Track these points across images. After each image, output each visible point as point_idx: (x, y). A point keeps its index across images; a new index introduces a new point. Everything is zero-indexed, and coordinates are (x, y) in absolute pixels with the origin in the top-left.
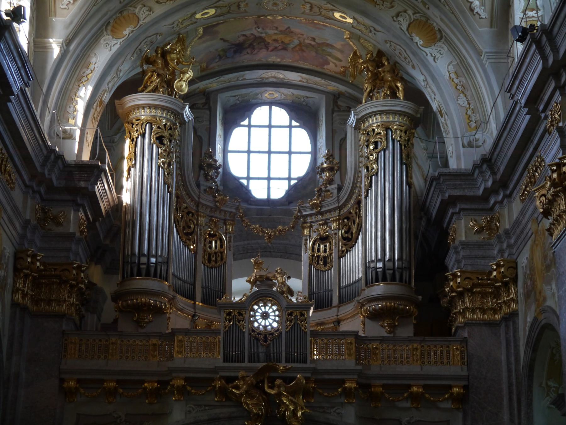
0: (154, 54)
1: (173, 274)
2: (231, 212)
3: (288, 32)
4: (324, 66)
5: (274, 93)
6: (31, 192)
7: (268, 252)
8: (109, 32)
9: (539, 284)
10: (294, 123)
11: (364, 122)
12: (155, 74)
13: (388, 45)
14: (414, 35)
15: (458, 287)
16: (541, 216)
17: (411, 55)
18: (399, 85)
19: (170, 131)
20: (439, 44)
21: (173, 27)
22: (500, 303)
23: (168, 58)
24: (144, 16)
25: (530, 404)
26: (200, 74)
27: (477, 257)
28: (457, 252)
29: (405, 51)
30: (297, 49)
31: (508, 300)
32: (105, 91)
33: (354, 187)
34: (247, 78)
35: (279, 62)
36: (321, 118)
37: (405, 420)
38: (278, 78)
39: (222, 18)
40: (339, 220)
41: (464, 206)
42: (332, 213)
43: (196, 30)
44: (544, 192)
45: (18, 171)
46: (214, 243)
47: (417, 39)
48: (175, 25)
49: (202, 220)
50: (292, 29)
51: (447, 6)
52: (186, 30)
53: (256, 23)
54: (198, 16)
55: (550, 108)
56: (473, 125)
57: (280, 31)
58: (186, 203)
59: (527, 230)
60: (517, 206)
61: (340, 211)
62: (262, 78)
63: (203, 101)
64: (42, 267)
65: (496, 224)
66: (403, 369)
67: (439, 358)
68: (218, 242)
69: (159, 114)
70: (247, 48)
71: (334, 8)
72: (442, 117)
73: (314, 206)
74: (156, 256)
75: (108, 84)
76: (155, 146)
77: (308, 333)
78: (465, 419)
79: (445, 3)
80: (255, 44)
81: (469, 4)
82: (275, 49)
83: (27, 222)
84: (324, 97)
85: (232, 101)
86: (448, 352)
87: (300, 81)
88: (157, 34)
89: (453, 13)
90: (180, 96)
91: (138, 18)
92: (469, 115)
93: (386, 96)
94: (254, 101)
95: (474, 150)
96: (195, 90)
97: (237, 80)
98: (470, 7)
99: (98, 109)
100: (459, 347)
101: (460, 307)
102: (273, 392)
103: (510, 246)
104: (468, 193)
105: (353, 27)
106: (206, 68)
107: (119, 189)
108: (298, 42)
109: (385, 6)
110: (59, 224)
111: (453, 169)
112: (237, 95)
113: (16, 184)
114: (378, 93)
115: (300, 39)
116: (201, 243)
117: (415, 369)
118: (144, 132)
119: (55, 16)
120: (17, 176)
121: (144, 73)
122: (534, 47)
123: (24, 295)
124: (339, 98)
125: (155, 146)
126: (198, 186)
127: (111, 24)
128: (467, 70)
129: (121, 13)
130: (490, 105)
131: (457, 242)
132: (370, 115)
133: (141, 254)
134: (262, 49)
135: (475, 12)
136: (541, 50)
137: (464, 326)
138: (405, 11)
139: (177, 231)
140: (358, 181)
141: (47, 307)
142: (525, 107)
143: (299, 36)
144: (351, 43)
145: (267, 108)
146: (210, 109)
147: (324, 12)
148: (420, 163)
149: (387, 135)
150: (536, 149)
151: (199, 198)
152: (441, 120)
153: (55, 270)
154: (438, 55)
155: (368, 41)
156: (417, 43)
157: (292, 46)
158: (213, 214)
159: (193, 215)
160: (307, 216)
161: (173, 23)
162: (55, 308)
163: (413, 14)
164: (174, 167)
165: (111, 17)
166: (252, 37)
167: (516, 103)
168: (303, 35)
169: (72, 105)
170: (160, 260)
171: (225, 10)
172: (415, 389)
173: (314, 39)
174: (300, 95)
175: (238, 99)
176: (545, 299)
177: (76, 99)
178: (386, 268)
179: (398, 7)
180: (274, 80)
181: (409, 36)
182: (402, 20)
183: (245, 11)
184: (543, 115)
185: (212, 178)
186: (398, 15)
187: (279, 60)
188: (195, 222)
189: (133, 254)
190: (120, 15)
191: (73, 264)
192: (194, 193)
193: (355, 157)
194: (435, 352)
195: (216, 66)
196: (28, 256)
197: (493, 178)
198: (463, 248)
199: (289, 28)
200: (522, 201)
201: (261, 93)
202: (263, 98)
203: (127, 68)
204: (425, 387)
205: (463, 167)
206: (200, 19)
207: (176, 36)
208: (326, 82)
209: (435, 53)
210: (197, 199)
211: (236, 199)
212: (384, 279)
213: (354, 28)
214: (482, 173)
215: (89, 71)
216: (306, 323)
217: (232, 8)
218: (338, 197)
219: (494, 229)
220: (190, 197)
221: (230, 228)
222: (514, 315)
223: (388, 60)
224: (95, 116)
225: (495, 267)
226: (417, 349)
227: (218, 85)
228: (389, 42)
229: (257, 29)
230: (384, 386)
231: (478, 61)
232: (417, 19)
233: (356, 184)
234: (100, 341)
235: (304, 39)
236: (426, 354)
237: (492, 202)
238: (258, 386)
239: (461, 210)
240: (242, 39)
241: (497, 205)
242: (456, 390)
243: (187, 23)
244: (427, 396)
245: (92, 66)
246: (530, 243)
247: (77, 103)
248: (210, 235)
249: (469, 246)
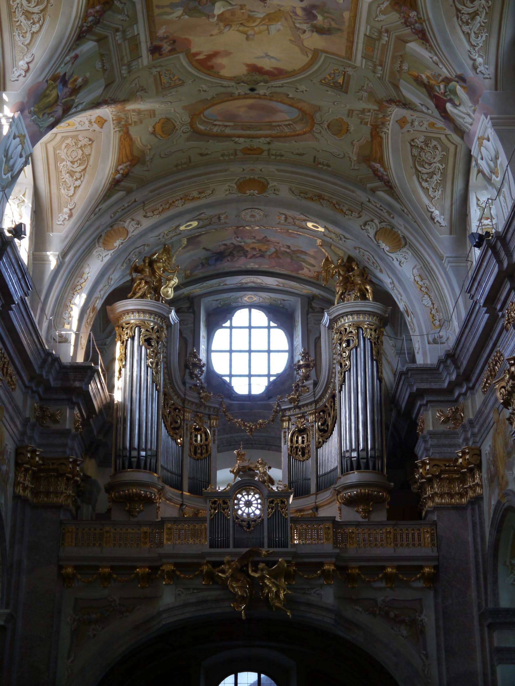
0: (142, 263)
1: (162, 467)
2: (215, 408)
3: (265, 241)
4: (298, 271)
6: (30, 392)
7: (250, 444)
8: (101, 244)
9: (501, 471)
10: (272, 324)
11: (336, 322)
12: (143, 282)
13: (357, 251)
14: (380, 242)
15: (427, 474)
16: (502, 406)
17: (378, 260)
18: (368, 287)
19: (157, 334)
20: (404, 250)
21: (160, 239)
22: (466, 488)
23: (155, 267)
24: (133, 229)
25: (495, 582)
26: (185, 281)
27: (444, 446)
28: (425, 442)
29: (373, 257)
30: (274, 256)
31: (474, 485)
32: (97, 298)
33: (328, 383)
35: (258, 268)
36: (297, 319)
37: (380, 599)
38: (258, 283)
39: (204, 229)
40: (315, 413)
41: (430, 398)
42: (309, 407)
43: (180, 241)
44: (503, 384)
45: (19, 373)
46: (199, 436)
47: (383, 245)
48: (161, 237)
49: (188, 416)
50: (269, 238)
51: (410, 216)
52: (171, 241)
53: (235, 233)
54: (182, 228)
55: (506, 307)
56: (437, 323)
57: (257, 240)
59: (489, 419)
60: (479, 397)
61: (316, 405)
62: (242, 283)
63: (187, 305)
64: (41, 462)
65: (460, 415)
66: (379, 552)
67: (411, 540)
68: (203, 435)
69: (147, 318)
70: (227, 256)
71: (307, 218)
72: (408, 316)
73: (291, 401)
74: (145, 450)
75: (100, 292)
76: (143, 348)
77: (289, 519)
78: (436, 597)
79: (408, 213)
80: (234, 252)
81: (430, 214)
82: (254, 256)
83: (27, 420)
84: (299, 300)
85: (214, 304)
86: (419, 535)
87: (277, 285)
88: (144, 245)
89: (415, 222)
90: (166, 301)
91: (128, 231)
93: (356, 298)
94: (234, 305)
95: (438, 346)
96: (180, 295)
97: (219, 286)
98: (431, 215)
99: (91, 315)
100: (429, 530)
101: (429, 492)
102: (256, 575)
103: (474, 435)
104: (434, 386)
105: (324, 235)
107: (111, 388)
109: (353, 216)
110: (56, 421)
111: (420, 364)
112: (219, 299)
113: (17, 386)
114: (349, 295)
115: (276, 247)
119: (52, 232)
120: (17, 377)
121: (133, 281)
122: (490, 252)
123: (25, 488)
125: (143, 348)
126: (184, 383)
127: (102, 237)
128: (430, 273)
129: (111, 227)
130: (452, 305)
131: (425, 432)
132: (342, 315)
133: (132, 447)
134: (241, 256)
135: (436, 220)
136: (496, 254)
137: (434, 509)
138: (372, 221)
139: (165, 426)
141: (46, 499)
142: (483, 306)
143: (276, 244)
144: (323, 250)
145: (247, 310)
146: (194, 312)
147: (297, 222)
148: (389, 358)
149: (358, 333)
150: (495, 345)
151: (185, 395)
152: (408, 319)
153: (53, 464)
154: (403, 260)
155: (339, 248)
156: (383, 249)
157: (268, 253)
158: (198, 410)
159: (180, 410)
160: (285, 410)
161: (159, 235)
162: (53, 499)
163: (380, 223)
164: (161, 366)
165: (103, 231)
166: (232, 246)
167: (476, 303)
168: (279, 243)
169: (67, 312)
170: (149, 453)
171: (206, 222)
172: (389, 570)
173: (289, 247)
174: (277, 299)
176: (507, 484)
177: (71, 306)
178: (360, 457)
179: (365, 217)
180: (253, 285)
181: (376, 242)
182: (369, 229)
183: (226, 223)
184: (500, 314)
185: (197, 377)
186: (365, 224)
187: (257, 266)
188: (182, 417)
189: (124, 448)
190: (111, 228)
191: (69, 458)
193: (329, 354)
194: (407, 535)
195: (199, 273)
196: (28, 452)
197: (457, 372)
198: (431, 438)
200: (484, 392)
201: (241, 297)
202: (244, 302)
203: (117, 277)
204: (398, 568)
205: (429, 362)
206: (184, 230)
207: (162, 246)
209: (400, 258)
210: (183, 396)
211: (219, 396)
212: (359, 468)
213: (326, 236)
214: (446, 367)
215: (83, 280)
216: (287, 510)
217: (213, 220)
218: (314, 392)
219: (459, 419)
220: (177, 394)
221: (214, 422)
222: (479, 498)
223: (357, 265)
224: (89, 321)
225: (460, 455)
226: (390, 532)
228: (358, 249)
229: (237, 239)
230: (360, 568)
231: (440, 265)
232: (383, 228)
234: (95, 529)
235: (280, 247)
236: (399, 537)
237: (456, 394)
238: (242, 570)
239: (428, 402)
240: (222, 248)
241: (461, 397)
242: (427, 570)
243: (171, 235)
244: (400, 576)
245: (85, 276)
246: (492, 431)
247: (72, 310)
248: (195, 429)
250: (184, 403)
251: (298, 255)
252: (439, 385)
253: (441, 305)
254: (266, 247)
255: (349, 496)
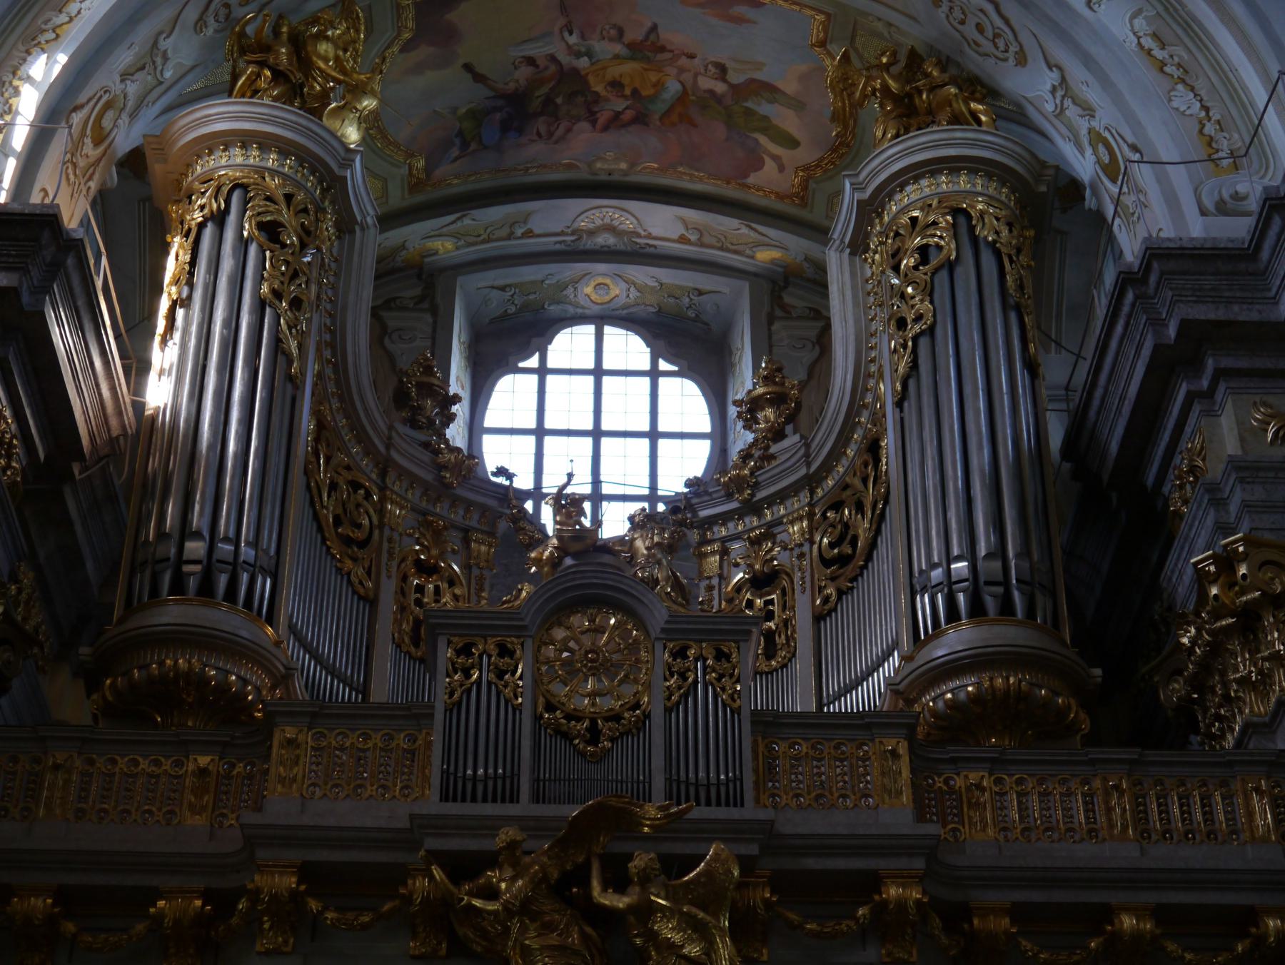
4: (746, 176)
5: (608, 281)
10: (663, 365)
33: (854, 408)
34: (537, 231)
35: (626, 174)
38: (624, 233)
57: (631, 46)
58: (349, 454)
61: (812, 492)
63: (417, 291)
76: (253, 250)
80: (559, 100)
82: (615, 121)
84: (745, 287)
87: (683, 240)
92: (1211, 138)
94: (554, 309)
97: (510, 236)
102: (621, 902)
104: (1241, 313)
106: (422, 176)
107: (138, 367)
108: (678, 87)
112: (510, 286)
116: (389, 577)
117: (1125, 853)
118: (223, 206)
124: (785, 287)
125: (253, 250)
128: (1187, 27)
134: (578, 119)
140: (867, 390)
145: (591, 329)
146: (434, 311)
151: (388, 447)
157: (660, 108)
160: (712, 521)
168: (692, 57)
172: (1128, 922)
173: (722, 70)
174: (681, 288)
175: (511, 301)
177: (16, 83)
178: (982, 579)
187: (623, 166)
192: (375, 428)
193: (857, 321)
198: (1242, 480)
199: (654, 28)
201: (575, 282)
202: (582, 300)
208: (752, 234)
215: (63, 18)
216: (738, 681)
227: (457, 248)
229: (566, 34)
230: (1018, 912)
233: (863, 397)
235: (696, 75)
239: (1220, 374)
240: (524, 72)
247: (17, 92)
248: (418, 562)
249: (1261, 474)
250: (383, 474)
251: (749, 104)
252: (1260, 312)
253: (1234, 112)
254: (653, 77)
255: (951, 705)
